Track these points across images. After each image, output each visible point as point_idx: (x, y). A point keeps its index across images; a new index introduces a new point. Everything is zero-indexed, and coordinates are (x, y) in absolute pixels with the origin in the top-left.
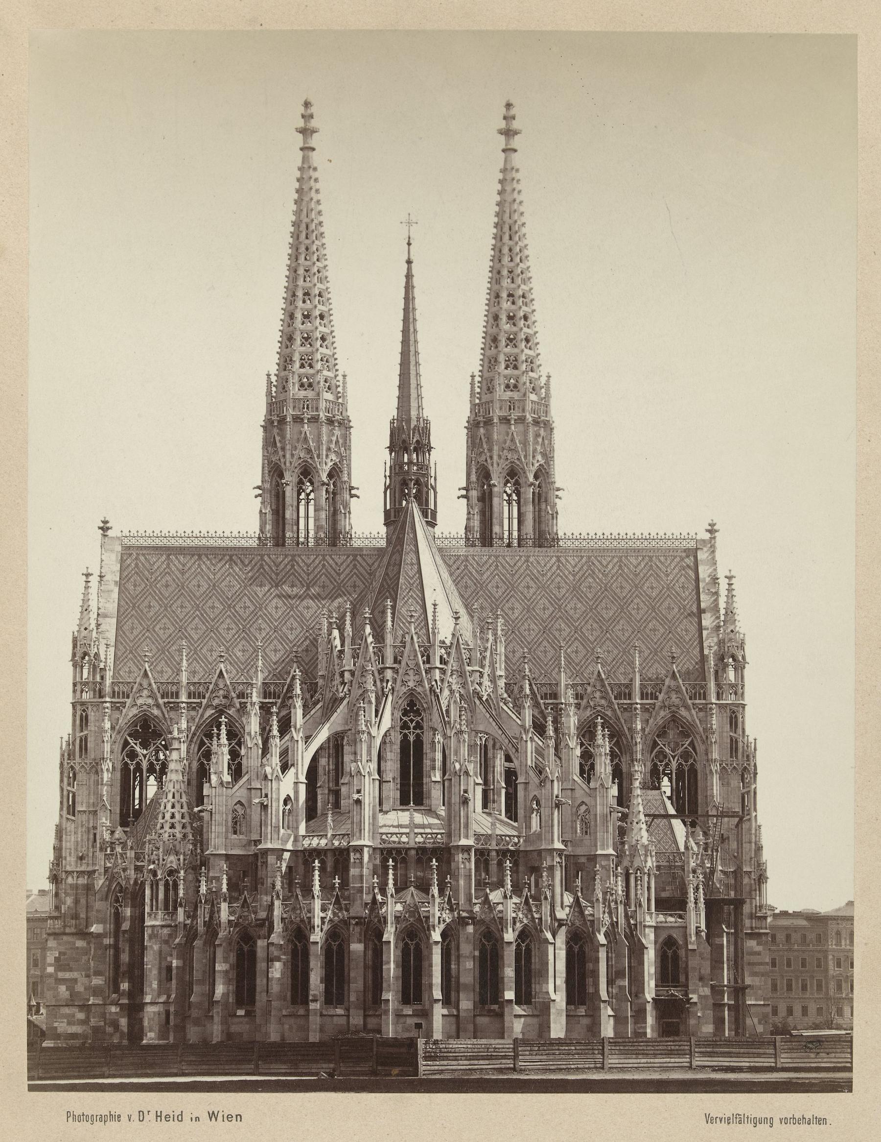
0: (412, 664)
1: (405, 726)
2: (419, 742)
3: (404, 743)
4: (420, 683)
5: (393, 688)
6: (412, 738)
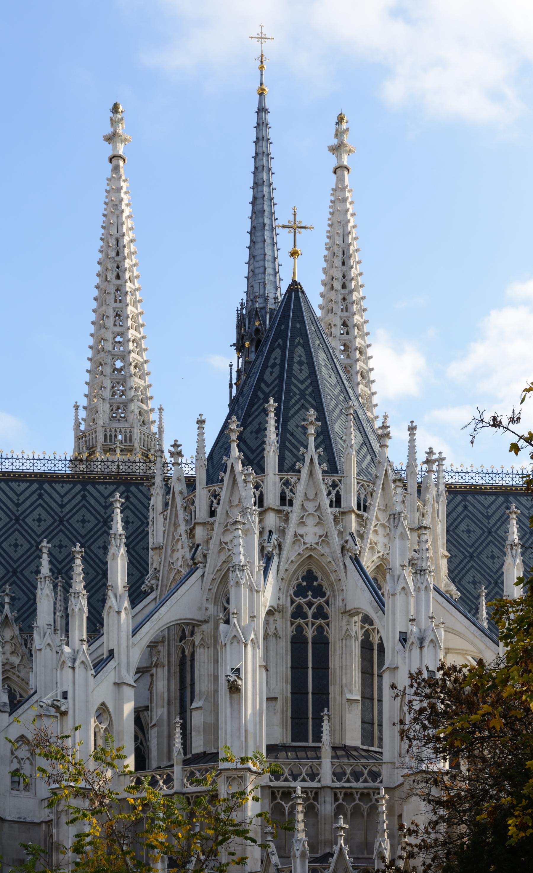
0: (311, 507)
1: (298, 613)
2: (322, 643)
3: (298, 642)
4: (325, 538)
6: (310, 633)
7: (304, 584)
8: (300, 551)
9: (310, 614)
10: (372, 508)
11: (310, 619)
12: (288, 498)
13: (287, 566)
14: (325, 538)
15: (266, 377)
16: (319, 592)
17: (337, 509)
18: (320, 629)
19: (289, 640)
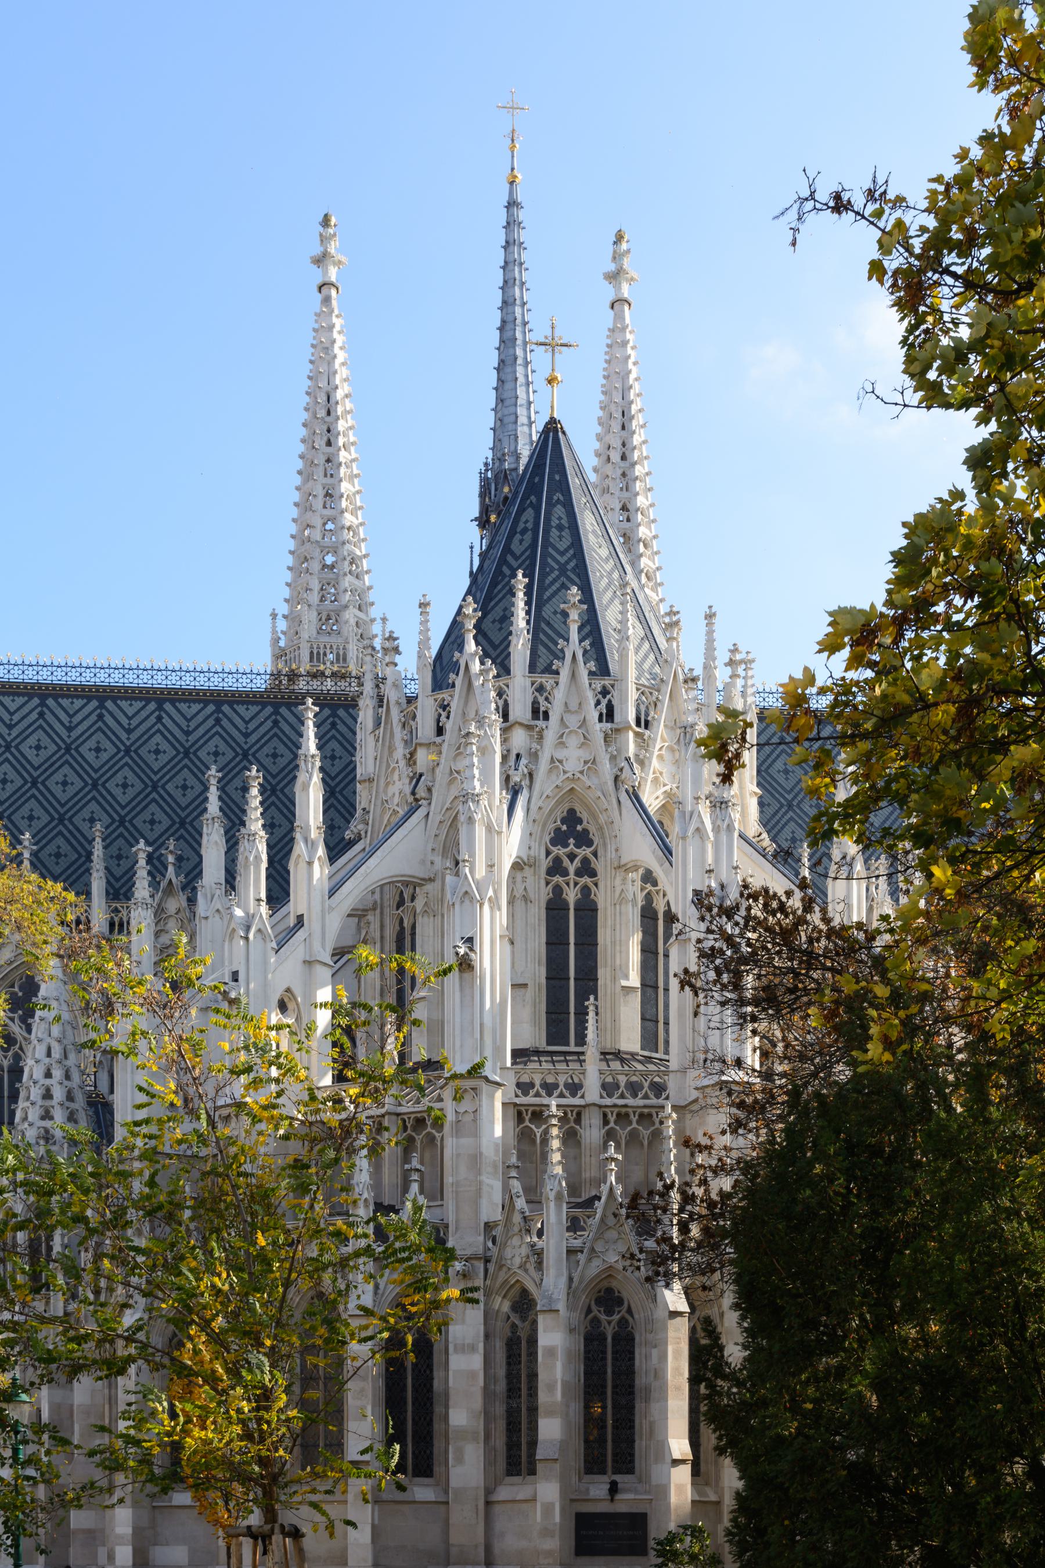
0: (573, 721)
1: (556, 868)
2: (588, 910)
3: (556, 908)
4: (592, 763)
6: (571, 896)
7: (564, 828)
8: (559, 782)
9: (572, 869)
10: (655, 723)
11: (572, 875)
12: (542, 709)
13: (540, 803)
14: (592, 763)
15: (513, 547)
16: (584, 839)
17: (609, 725)
18: (586, 891)
19: (543, 905)
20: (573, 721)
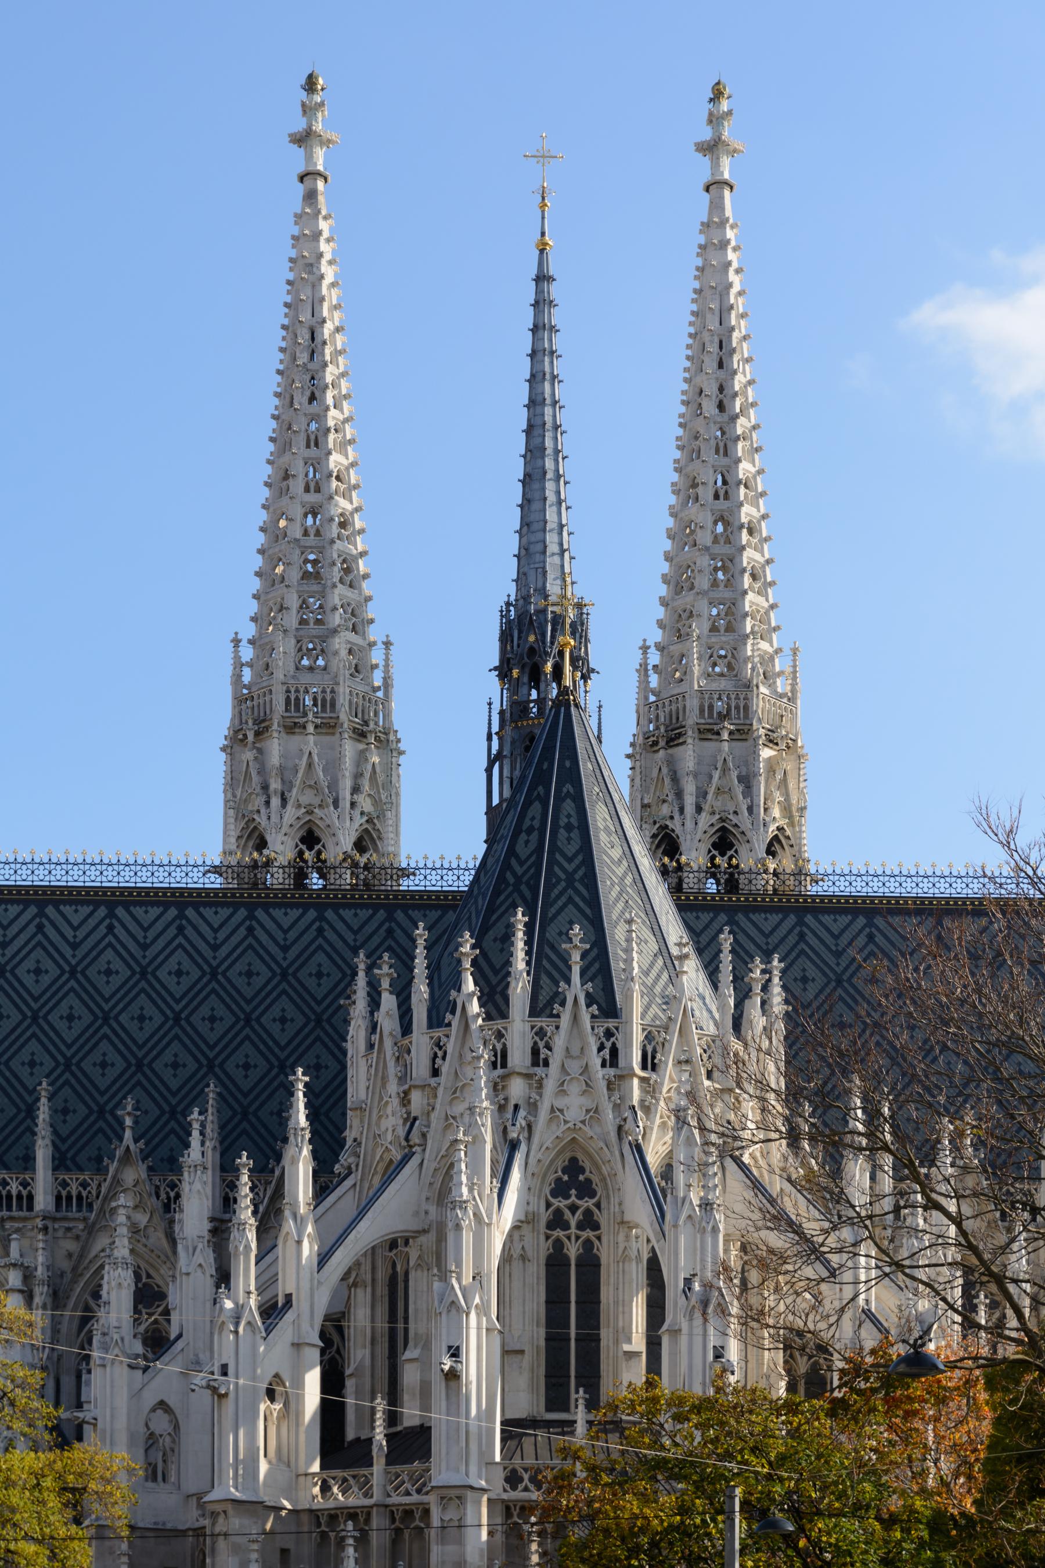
0: (575, 1067)
3: (556, 1263)
5: (530, 1126)
6: (573, 1251)
9: (573, 1223)
11: (573, 1230)
17: (612, 1072)
19: (543, 1261)
20: (575, 1067)
